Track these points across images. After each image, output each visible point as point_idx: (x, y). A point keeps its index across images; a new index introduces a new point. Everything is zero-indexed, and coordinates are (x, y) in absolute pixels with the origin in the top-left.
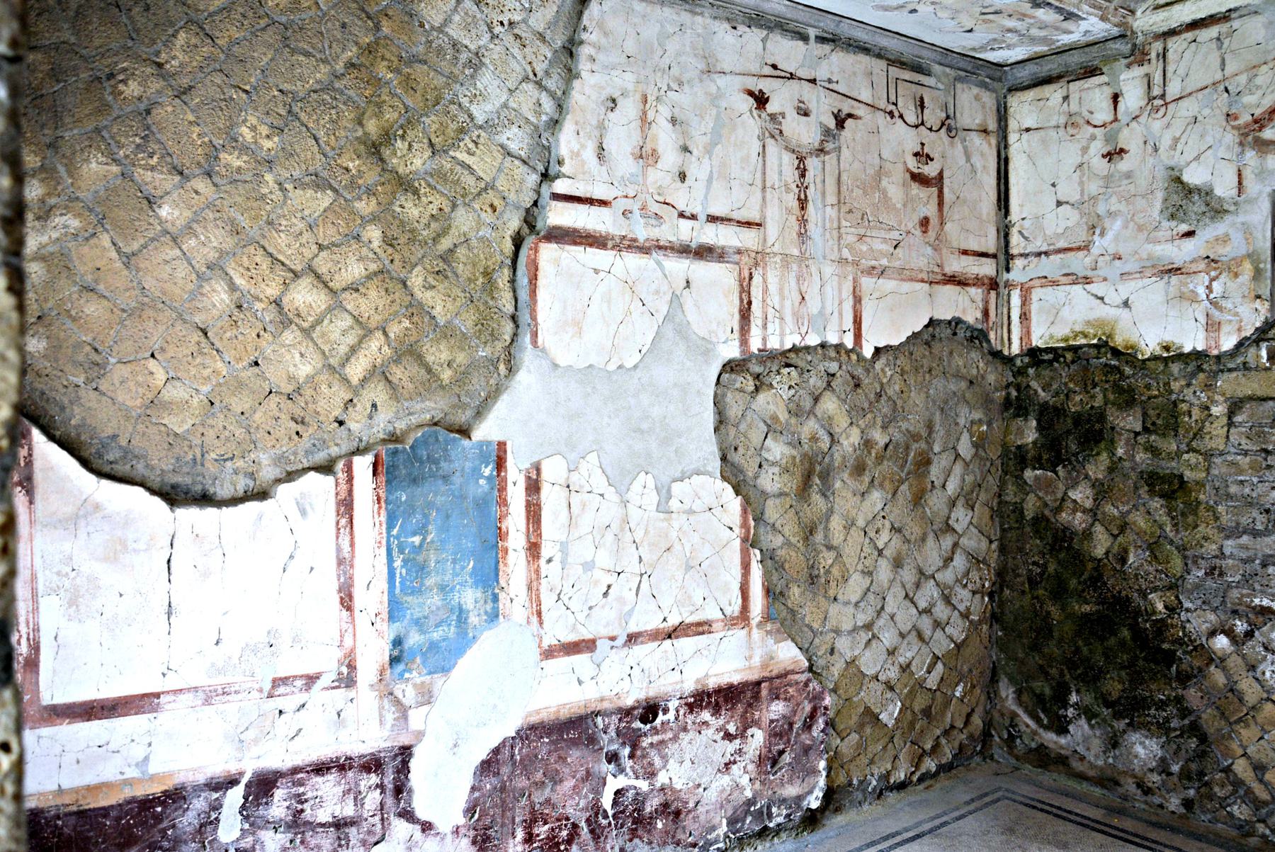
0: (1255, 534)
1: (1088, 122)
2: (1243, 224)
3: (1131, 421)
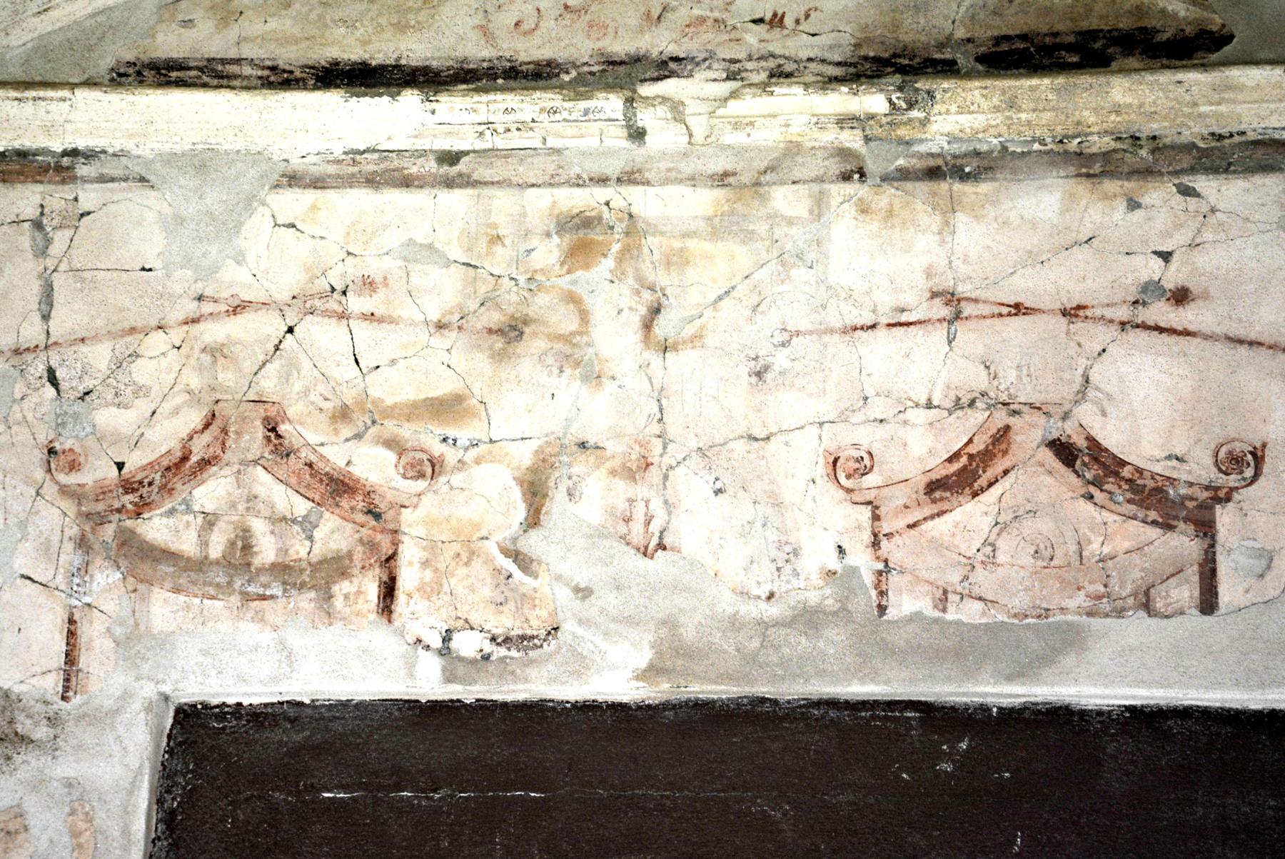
2: (69, 784)
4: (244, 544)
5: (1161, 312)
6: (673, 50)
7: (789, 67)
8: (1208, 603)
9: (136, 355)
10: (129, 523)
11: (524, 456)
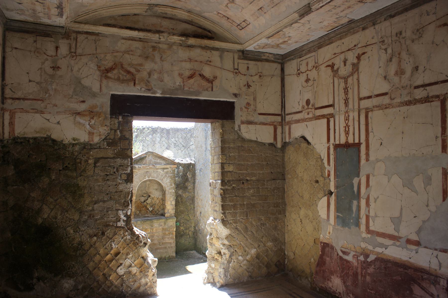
0: (104, 202)
1: (45, 53)
3: (58, 166)
4: (119, 77)
5: (208, 63)
6: (163, 30)
7: (175, 34)
8: (212, 90)
9: (106, 56)
10: (106, 74)
11: (148, 70)
